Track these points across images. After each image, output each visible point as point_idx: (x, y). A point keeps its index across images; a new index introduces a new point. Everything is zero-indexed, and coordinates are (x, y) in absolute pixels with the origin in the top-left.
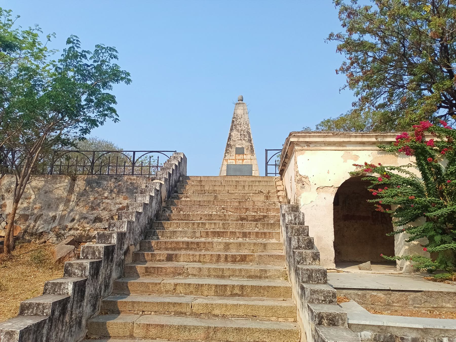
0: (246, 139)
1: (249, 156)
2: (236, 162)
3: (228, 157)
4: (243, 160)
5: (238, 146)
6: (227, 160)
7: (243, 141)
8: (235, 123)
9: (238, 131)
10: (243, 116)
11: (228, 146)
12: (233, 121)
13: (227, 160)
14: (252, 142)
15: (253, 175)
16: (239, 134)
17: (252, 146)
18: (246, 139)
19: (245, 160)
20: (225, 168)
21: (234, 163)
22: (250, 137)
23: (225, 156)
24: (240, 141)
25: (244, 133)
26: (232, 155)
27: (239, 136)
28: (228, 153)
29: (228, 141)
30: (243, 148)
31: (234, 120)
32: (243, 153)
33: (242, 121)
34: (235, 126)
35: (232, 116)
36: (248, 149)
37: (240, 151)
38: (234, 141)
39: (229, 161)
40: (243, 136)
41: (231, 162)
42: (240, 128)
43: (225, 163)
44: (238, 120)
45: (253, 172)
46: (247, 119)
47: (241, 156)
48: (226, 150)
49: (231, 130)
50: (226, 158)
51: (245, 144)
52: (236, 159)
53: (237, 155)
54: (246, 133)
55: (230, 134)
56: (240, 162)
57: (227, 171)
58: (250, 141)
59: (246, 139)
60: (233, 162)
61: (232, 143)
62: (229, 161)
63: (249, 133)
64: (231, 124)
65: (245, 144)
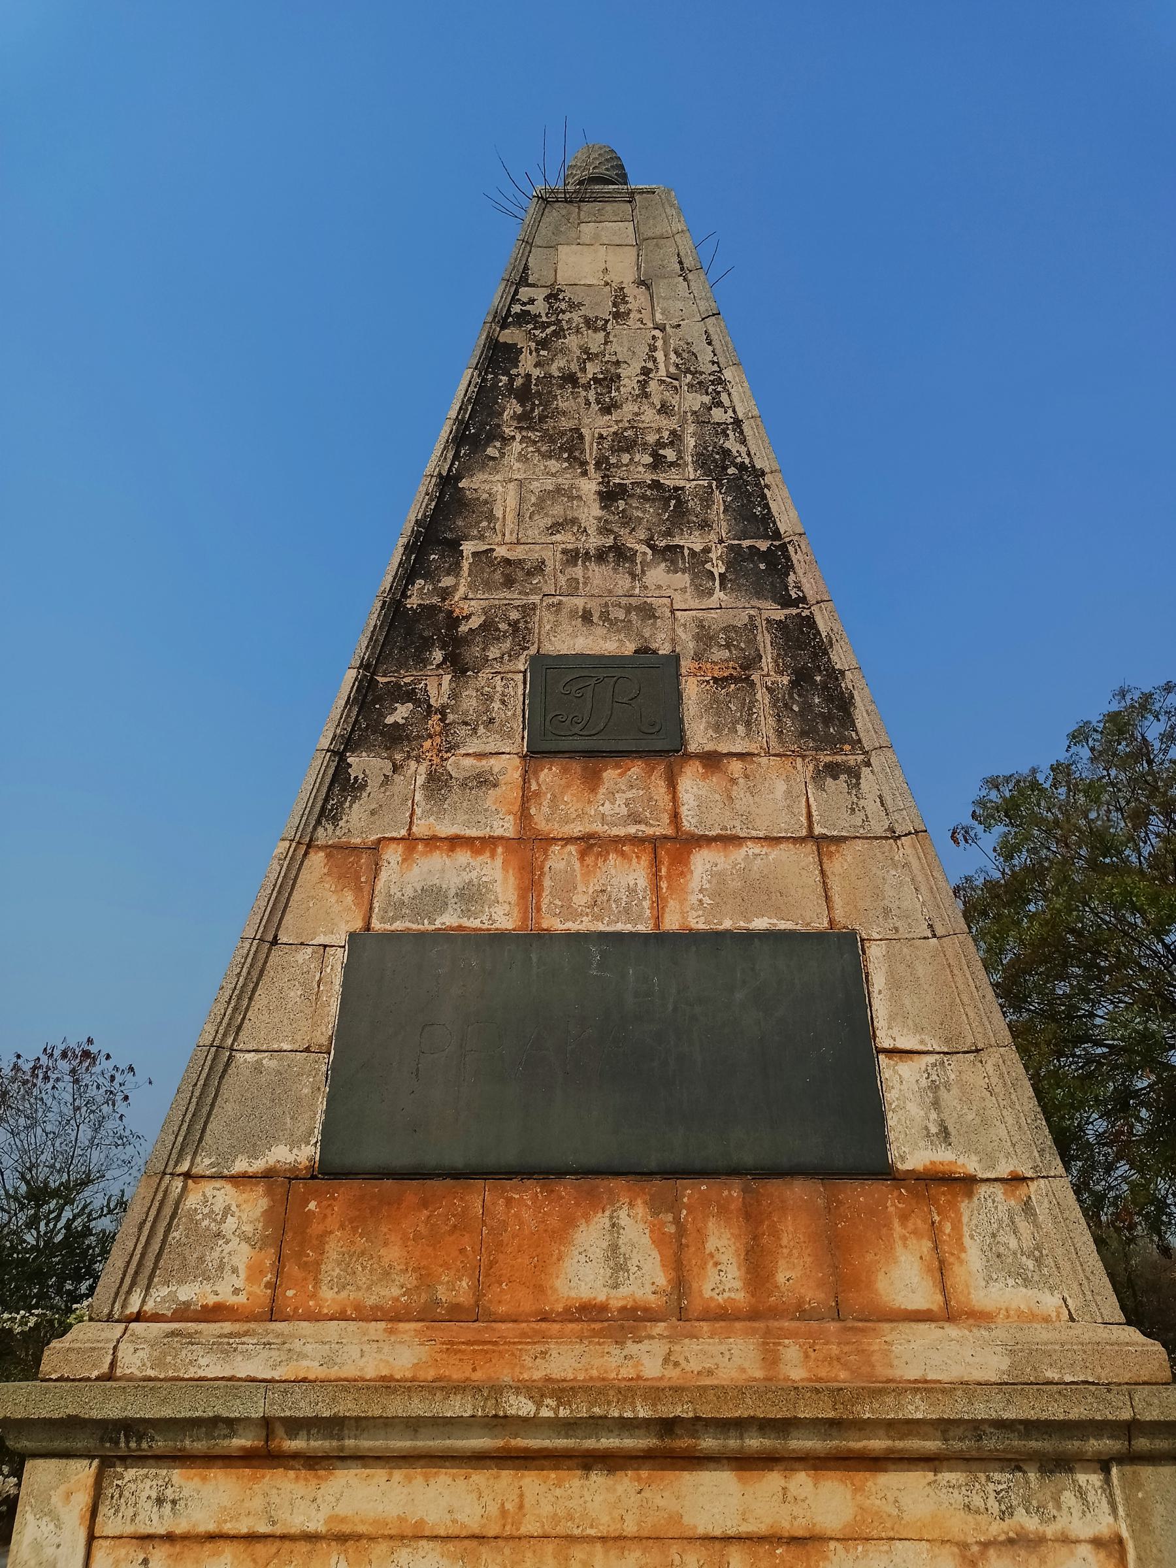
0: (693, 541)
1: (778, 792)
2: (530, 885)
3: (391, 797)
4: (672, 848)
5: (569, 641)
6: (358, 864)
7: (658, 575)
8: (527, 364)
9: (569, 448)
10: (637, 298)
11: (411, 633)
12: (498, 356)
13: (358, 864)
14: (805, 578)
15: (911, 1151)
16: (589, 486)
17: (801, 640)
18: (712, 539)
19: (702, 861)
20: (302, 1010)
21: (502, 916)
22: (751, 510)
23: (341, 785)
24: (599, 575)
25: (670, 479)
26: (460, 765)
27: (591, 512)
28: (395, 737)
29: (410, 573)
30: (655, 673)
31: (509, 336)
32: (659, 743)
33: (627, 346)
34: (523, 395)
35: (495, 297)
36: (741, 677)
37: (606, 716)
38: (512, 573)
39: (400, 876)
40: (647, 513)
41: (433, 898)
42: (595, 425)
43: (328, 915)
44: (572, 342)
45: (901, 1084)
46: (693, 331)
47: (621, 797)
48: (368, 697)
49: (474, 437)
50: (357, 821)
51: (686, 608)
52: (528, 847)
53: (548, 775)
54: (686, 478)
55: (447, 482)
56: (607, 897)
57: (356, 1062)
58: (764, 565)
59: (693, 541)
60: (471, 896)
61: (470, 601)
62: (400, 876)
63: (746, 491)
64: (464, 381)
65: (686, 608)
